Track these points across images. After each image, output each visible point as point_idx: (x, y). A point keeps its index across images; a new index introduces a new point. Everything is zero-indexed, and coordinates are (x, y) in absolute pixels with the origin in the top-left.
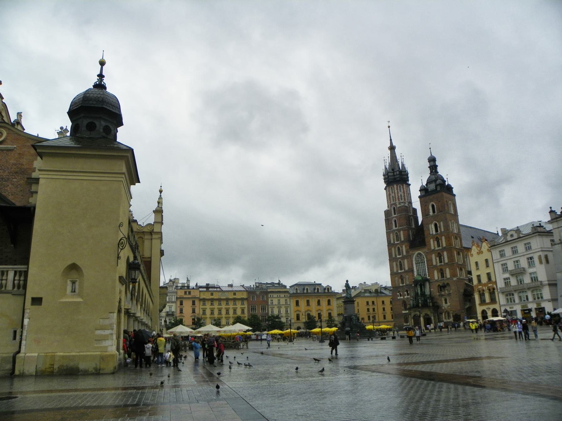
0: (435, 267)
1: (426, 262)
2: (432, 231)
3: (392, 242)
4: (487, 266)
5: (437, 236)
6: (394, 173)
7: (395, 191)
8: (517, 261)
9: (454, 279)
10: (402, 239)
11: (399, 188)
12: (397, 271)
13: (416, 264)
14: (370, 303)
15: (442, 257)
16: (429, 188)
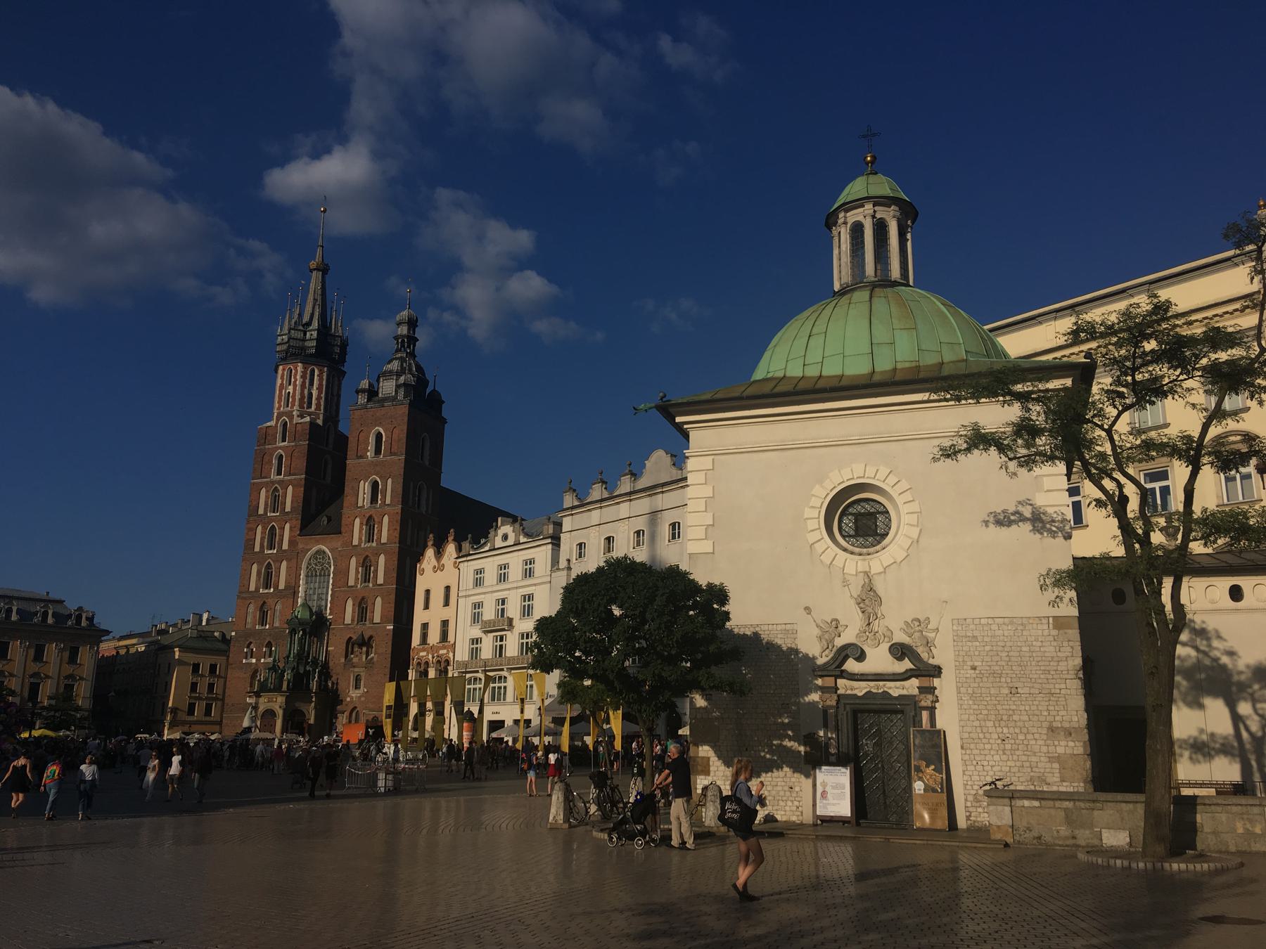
4: (447, 603)
6: (305, 334)
7: (296, 380)
9: (388, 628)
10: (288, 509)
11: (308, 376)
12: (257, 589)
13: (307, 576)
15: (372, 568)
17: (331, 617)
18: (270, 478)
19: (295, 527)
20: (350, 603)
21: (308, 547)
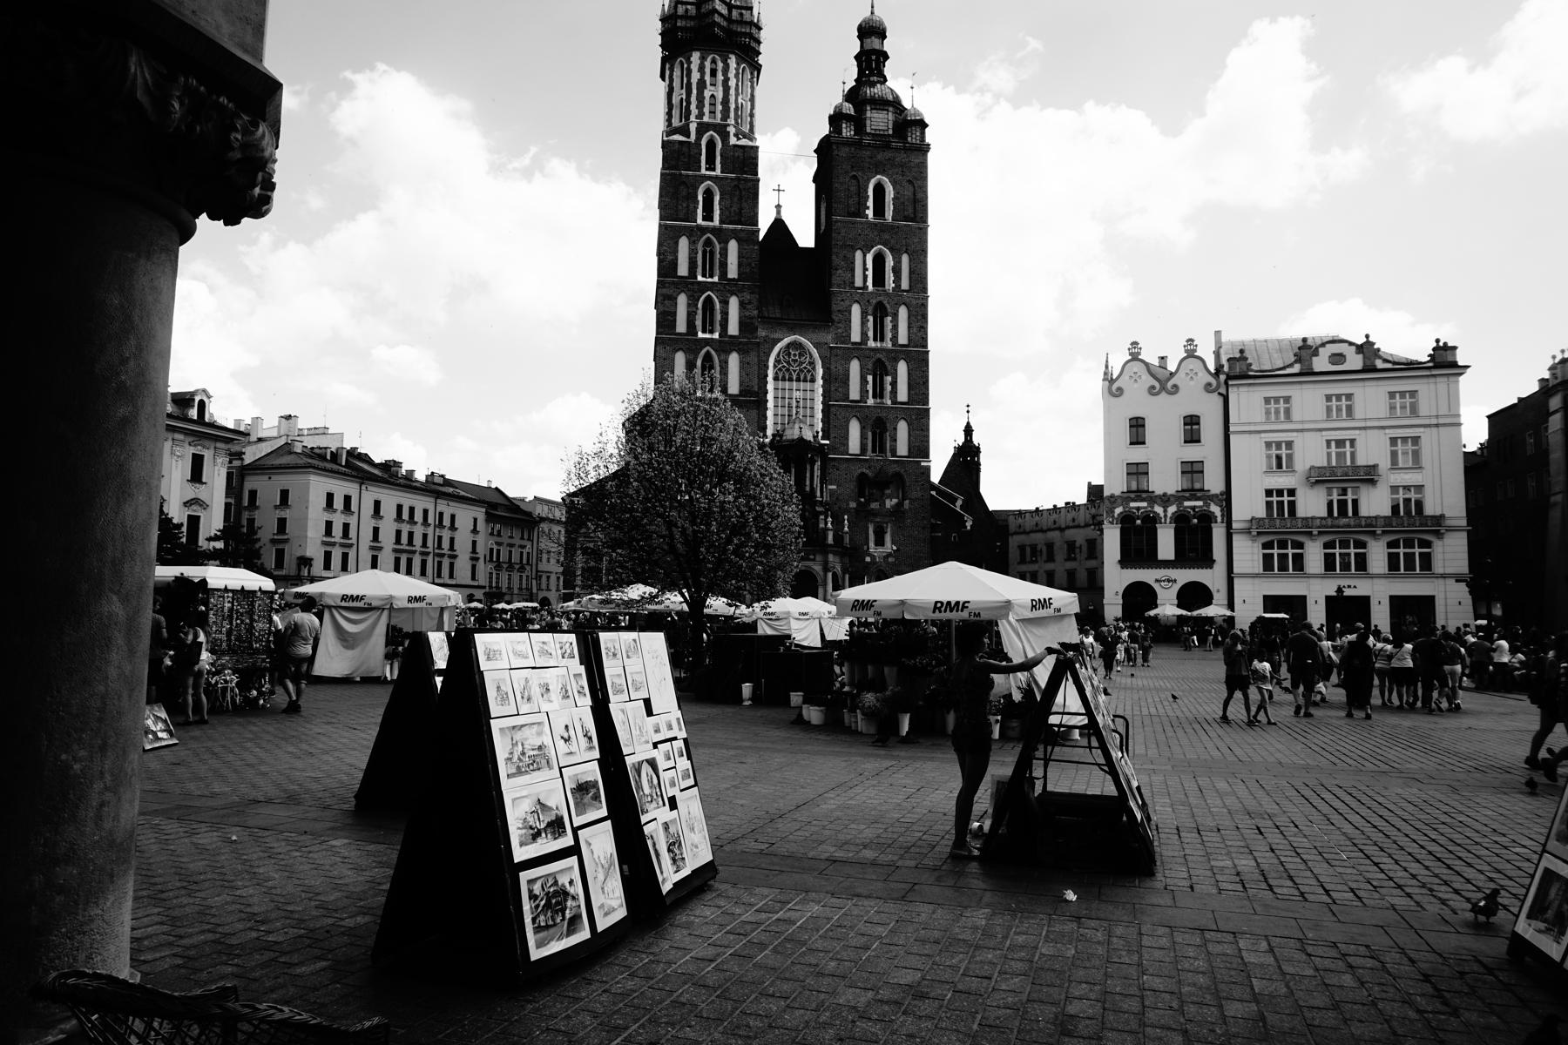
0: (857, 409)
1: (821, 382)
2: (865, 277)
3: (683, 270)
5: (882, 298)
7: (726, 80)
8: (1340, 443)
9: (923, 464)
10: (733, 272)
13: (776, 379)
14: (338, 503)
15: (889, 379)
16: (868, 122)
17: (827, 442)
18: (696, 221)
19: (750, 303)
20: (854, 429)
21: (780, 336)
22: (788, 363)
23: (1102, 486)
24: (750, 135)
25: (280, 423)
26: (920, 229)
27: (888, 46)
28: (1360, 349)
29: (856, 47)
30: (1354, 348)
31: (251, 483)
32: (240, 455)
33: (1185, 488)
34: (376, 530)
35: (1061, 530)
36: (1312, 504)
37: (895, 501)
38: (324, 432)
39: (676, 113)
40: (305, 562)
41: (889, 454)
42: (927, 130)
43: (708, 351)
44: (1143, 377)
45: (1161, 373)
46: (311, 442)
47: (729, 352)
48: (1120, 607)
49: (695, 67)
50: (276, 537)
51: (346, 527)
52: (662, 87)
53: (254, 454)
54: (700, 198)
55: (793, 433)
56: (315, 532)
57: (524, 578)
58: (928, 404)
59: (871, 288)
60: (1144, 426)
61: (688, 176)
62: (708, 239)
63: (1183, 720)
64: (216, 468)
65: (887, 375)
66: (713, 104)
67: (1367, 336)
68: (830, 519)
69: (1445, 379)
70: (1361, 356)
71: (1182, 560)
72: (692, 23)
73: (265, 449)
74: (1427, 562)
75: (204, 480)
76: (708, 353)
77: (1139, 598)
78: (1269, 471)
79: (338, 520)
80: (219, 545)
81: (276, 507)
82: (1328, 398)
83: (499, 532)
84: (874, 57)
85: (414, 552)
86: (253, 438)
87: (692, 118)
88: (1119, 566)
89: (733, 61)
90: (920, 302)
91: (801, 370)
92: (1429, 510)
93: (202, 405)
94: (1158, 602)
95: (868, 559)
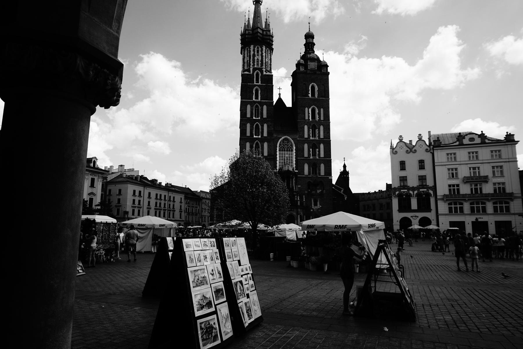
0: (307, 160)
1: (295, 151)
2: (309, 116)
3: (248, 115)
5: (314, 123)
8: (474, 168)
9: (329, 178)
10: (265, 116)
13: (280, 150)
14: (137, 194)
16: (309, 66)
17: (297, 171)
19: (271, 126)
21: (281, 136)
22: (284, 145)
23: (391, 184)
24: (271, 72)
25: (119, 167)
26: (327, 100)
27: (315, 41)
28: (480, 136)
29: (304, 42)
30: (477, 136)
31: (109, 187)
32: (106, 178)
33: (420, 184)
34: (149, 202)
35: (378, 199)
36: (465, 189)
37: (320, 190)
38: (132, 170)
39: (246, 65)
40: (127, 213)
41: (318, 175)
42: (328, 68)
43: (257, 142)
44: (404, 147)
45: (410, 146)
46: (128, 174)
47: (264, 142)
48: (399, 226)
49: (252, 50)
50: (117, 205)
51: (139, 201)
52: (241, 57)
53: (111, 178)
54: (254, 92)
55: (286, 168)
56: (129, 203)
57: (197, 218)
58: (331, 158)
59: (311, 120)
60: (405, 164)
61: (250, 85)
62: (257, 105)
63: (423, 266)
64: (99, 182)
65: (317, 149)
66: (258, 62)
67: (482, 132)
68: (298, 197)
69: (510, 146)
70: (480, 138)
71: (420, 209)
72: (251, 36)
73: (114, 176)
74: (508, 209)
75: (95, 186)
76: (257, 143)
77: (405, 223)
78: (449, 178)
79: (137, 199)
80: (99, 207)
81: (117, 195)
82: (469, 153)
83: (189, 202)
84: (310, 45)
85: (161, 209)
86: (110, 173)
87: (251, 66)
88: (398, 212)
89: (264, 48)
90: (328, 124)
91: (288, 148)
92: (508, 191)
93: (95, 162)
94: (412, 224)
95: (312, 210)
